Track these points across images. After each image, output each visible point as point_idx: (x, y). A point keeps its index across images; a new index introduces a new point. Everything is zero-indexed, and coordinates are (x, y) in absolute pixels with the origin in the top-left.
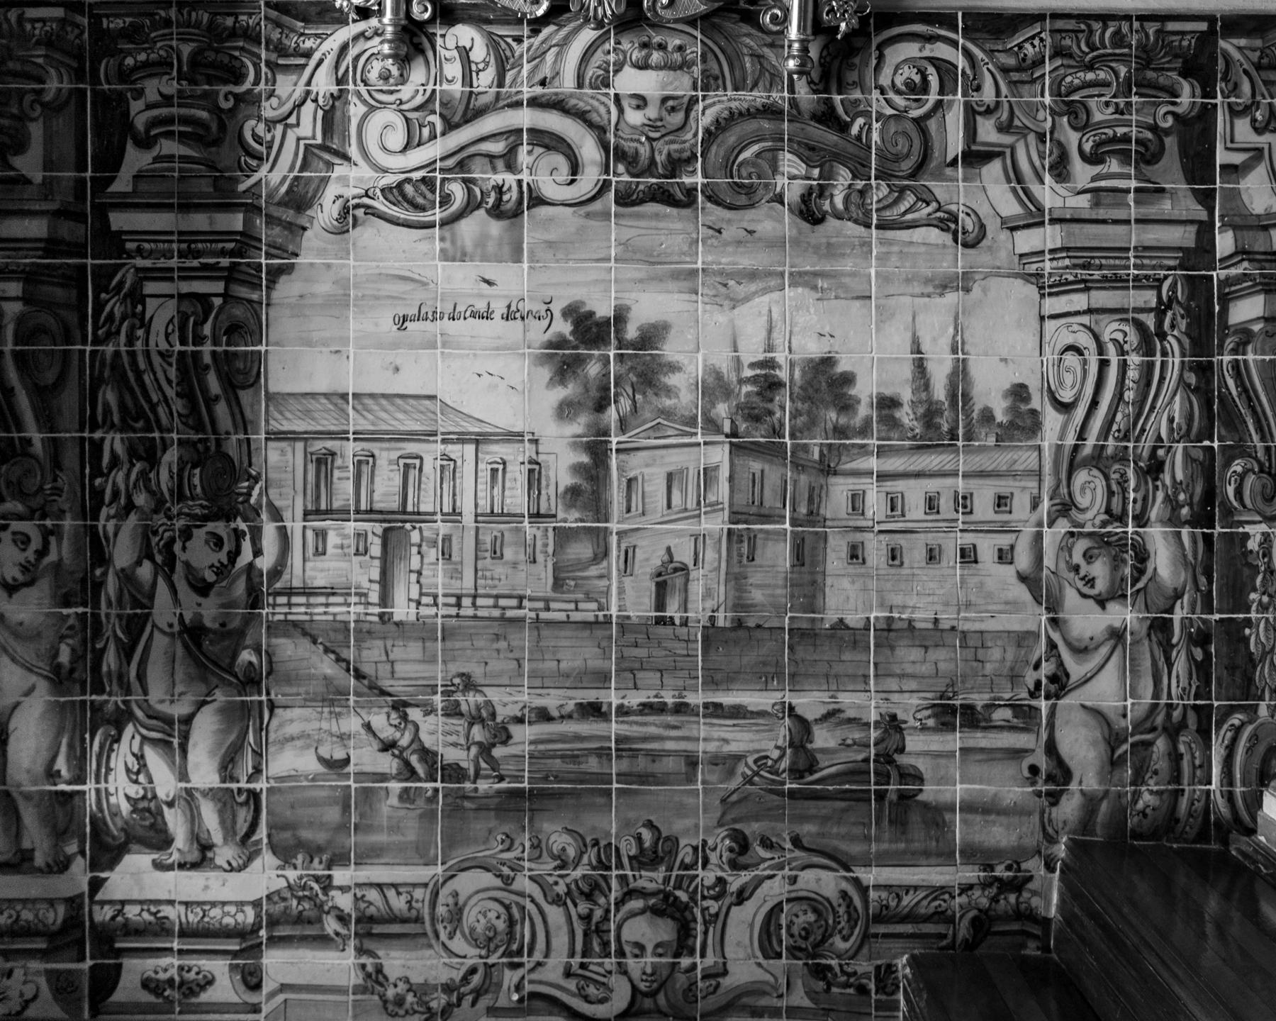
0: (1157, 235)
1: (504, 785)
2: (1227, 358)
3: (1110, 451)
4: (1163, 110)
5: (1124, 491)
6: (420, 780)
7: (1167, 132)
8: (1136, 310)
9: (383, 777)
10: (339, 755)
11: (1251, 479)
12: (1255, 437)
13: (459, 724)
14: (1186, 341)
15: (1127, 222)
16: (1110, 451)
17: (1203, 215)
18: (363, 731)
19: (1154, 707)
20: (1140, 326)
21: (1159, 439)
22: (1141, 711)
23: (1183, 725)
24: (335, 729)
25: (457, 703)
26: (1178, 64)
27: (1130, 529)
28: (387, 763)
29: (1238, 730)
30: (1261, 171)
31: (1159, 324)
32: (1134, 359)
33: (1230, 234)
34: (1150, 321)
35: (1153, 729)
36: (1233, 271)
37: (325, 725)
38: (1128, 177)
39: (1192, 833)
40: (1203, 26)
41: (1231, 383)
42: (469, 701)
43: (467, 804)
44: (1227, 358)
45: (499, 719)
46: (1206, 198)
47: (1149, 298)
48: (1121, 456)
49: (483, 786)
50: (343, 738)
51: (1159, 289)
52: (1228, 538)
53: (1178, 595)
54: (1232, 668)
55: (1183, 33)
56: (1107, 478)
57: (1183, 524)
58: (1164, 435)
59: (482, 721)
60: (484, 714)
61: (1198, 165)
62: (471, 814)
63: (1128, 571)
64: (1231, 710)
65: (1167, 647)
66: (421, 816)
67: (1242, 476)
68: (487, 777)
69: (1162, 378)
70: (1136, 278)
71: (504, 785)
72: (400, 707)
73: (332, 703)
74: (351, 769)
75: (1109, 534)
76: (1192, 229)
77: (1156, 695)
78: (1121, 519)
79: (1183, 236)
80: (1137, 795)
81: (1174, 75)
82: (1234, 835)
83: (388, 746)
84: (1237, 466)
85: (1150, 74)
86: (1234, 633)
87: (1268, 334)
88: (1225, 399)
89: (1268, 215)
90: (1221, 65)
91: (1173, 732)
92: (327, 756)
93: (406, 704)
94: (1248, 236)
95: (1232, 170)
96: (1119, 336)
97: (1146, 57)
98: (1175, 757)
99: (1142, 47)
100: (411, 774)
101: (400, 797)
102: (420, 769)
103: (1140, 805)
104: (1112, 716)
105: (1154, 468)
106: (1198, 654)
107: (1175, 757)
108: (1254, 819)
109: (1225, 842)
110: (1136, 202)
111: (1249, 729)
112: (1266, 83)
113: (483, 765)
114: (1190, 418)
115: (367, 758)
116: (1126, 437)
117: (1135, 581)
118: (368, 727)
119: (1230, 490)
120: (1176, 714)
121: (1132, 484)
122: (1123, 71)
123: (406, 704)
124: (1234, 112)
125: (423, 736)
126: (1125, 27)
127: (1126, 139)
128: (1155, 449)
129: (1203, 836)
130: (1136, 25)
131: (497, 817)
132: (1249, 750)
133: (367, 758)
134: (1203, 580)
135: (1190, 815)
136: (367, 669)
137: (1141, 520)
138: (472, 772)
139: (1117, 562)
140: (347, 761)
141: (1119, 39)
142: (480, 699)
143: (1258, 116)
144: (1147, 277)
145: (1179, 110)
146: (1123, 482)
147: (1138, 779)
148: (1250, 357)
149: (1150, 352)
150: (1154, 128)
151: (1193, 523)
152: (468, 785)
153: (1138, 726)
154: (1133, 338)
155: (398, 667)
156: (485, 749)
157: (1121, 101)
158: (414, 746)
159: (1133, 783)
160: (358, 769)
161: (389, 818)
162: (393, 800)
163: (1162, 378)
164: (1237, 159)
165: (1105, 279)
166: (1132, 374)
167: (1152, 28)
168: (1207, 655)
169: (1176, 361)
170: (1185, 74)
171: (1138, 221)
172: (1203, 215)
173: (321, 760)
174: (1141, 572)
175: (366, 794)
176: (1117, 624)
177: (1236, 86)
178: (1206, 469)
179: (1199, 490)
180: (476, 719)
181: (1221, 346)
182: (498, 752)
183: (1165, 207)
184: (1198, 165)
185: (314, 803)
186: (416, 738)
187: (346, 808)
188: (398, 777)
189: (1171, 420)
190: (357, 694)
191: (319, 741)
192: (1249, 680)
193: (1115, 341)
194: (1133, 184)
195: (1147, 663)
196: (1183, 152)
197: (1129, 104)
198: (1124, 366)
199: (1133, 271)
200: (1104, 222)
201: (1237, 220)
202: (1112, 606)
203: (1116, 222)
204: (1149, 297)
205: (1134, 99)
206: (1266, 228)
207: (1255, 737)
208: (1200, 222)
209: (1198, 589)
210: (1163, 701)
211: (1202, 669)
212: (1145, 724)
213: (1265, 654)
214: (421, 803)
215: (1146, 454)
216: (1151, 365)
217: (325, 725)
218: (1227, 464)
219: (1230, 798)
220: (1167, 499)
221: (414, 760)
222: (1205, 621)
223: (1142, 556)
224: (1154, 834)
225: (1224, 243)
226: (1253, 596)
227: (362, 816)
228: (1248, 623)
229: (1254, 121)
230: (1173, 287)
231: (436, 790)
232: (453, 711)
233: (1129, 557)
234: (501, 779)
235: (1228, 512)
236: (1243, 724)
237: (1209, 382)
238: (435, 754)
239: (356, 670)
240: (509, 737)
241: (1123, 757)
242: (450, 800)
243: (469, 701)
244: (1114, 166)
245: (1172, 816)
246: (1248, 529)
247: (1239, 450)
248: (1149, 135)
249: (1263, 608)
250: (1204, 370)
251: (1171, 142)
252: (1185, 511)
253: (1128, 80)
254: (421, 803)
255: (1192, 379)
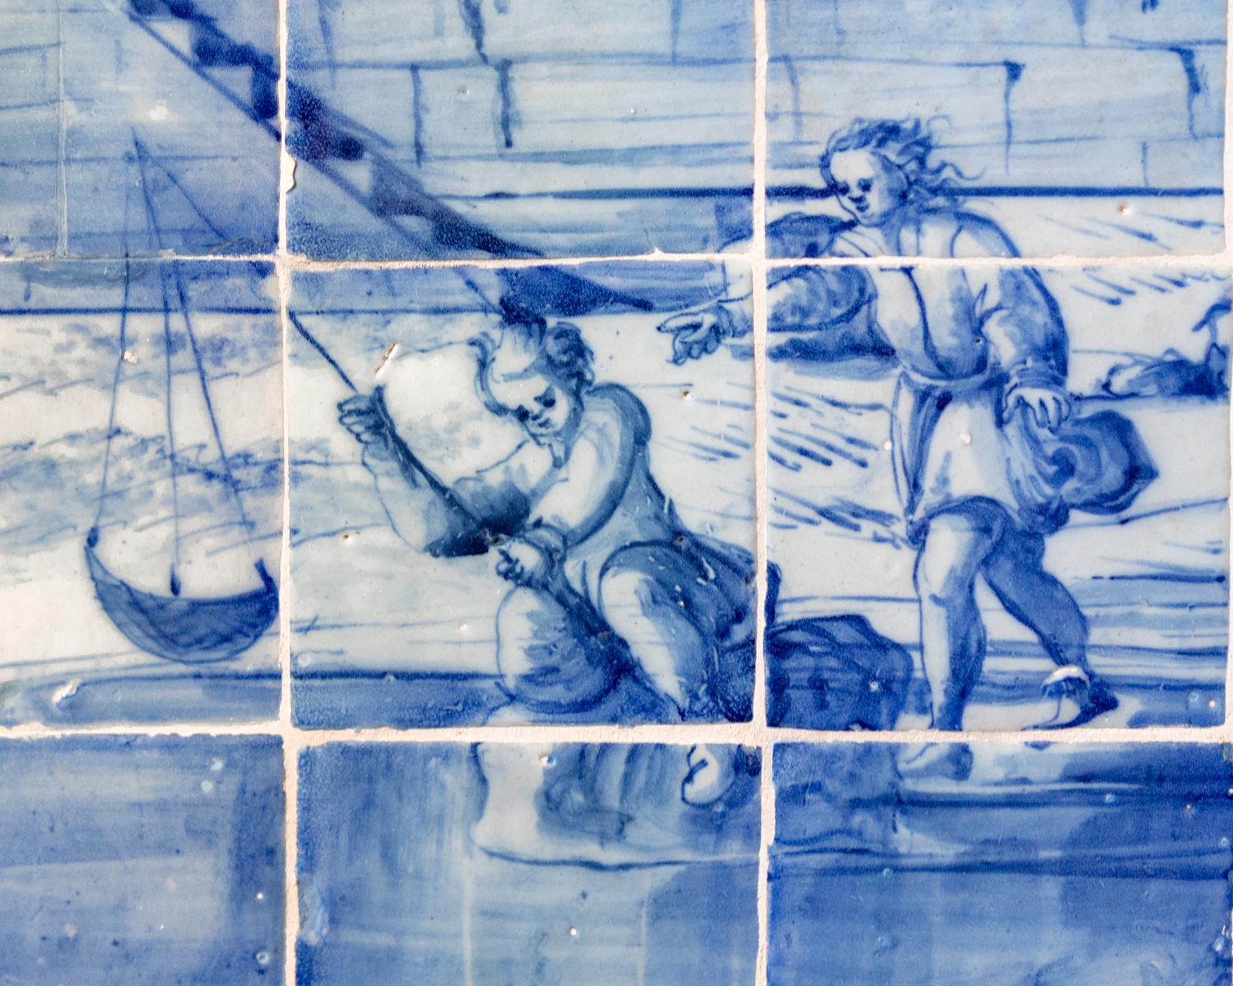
1: (1109, 735)
6: (652, 707)
9: (454, 695)
10: (217, 573)
13: (872, 402)
18: (343, 445)
24: (190, 430)
25: (858, 291)
28: (482, 620)
37: (139, 413)
42: (923, 276)
43: (913, 840)
45: (1084, 375)
49: (1001, 739)
50: (235, 478)
59: (994, 383)
60: (1004, 346)
62: (936, 896)
66: (663, 906)
68: (1020, 691)
71: (1109, 735)
72: (547, 305)
73: (175, 289)
74: (280, 647)
83: (482, 527)
92: (152, 582)
93: (579, 296)
100: (613, 677)
101: (551, 804)
102: (658, 650)
113: (999, 624)
115: (370, 590)
118: (372, 418)
123: (579, 296)
125: (670, 465)
131: (1076, 910)
133: (370, 590)
136: (361, 102)
138: (936, 665)
140: (261, 605)
142: (982, 264)
152: (915, 736)
155: (535, 93)
156: (1010, 541)
158: (626, 524)
160: (320, 650)
161: (490, 913)
162: (514, 821)
173: (119, 600)
175: (364, 789)
180: (958, 376)
182: (1080, 553)
185: (77, 838)
186: (634, 476)
187: (254, 862)
188: (537, 694)
190: (316, 240)
191: (108, 498)
214: (660, 832)
217: (139, 413)
221: (623, 598)
227: (340, 906)
231: (744, 765)
232: (837, 334)
234: (1097, 700)
238: (737, 566)
239: (307, 108)
240: (1139, 472)
242: (817, 817)
243: (923, 276)
254: (660, 832)
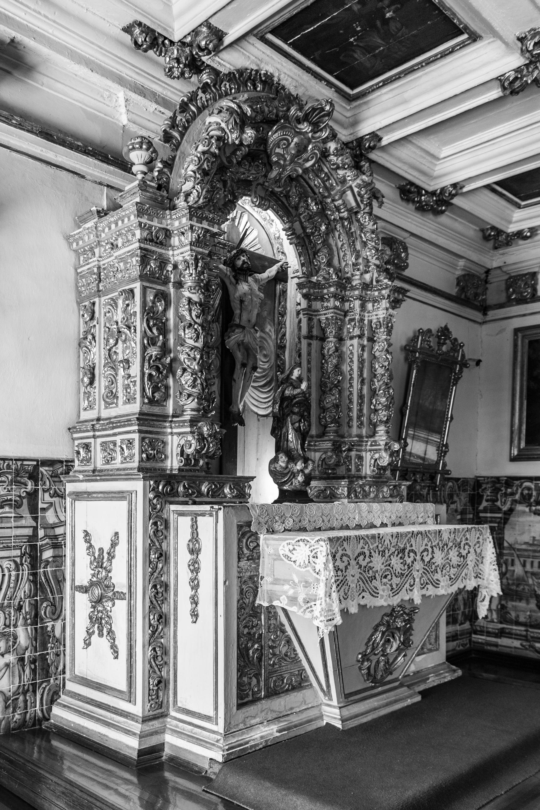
0: (20, 532)
2: (42, 570)
3: (5, 604)
4: (23, 490)
5: (10, 617)
7: (24, 498)
8: (14, 557)
11: (49, 608)
12: (50, 595)
14: (29, 566)
15: (11, 528)
16: (5, 604)
17: (35, 525)
19: (19, 686)
20: (15, 562)
21: (21, 598)
22: (15, 689)
23: (28, 690)
26: (27, 475)
27: (12, 629)
29: (44, 688)
30: (52, 510)
31: (21, 561)
32: (13, 573)
33: (43, 530)
34: (18, 560)
35: (19, 694)
36: (44, 542)
38: (11, 513)
39: (30, 724)
40: (35, 463)
41: (43, 578)
44: (42, 570)
46: (35, 519)
47: (18, 553)
48: (9, 606)
51: (21, 549)
52: (42, 628)
53: (27, 649)
54: (43, 669)
55: (29, 465)
56: (4, 613)
57: (28, 625)
58: (23, 597)
61: (34, 509)
63: (11, 643)
64: (43, 682)
65: (23, 666)
67: (46, 608)
69: (22, 579)
70: (14, 546)
75: (5, 632)
76: (32, 529)
77: (20, 682)
78: (9, 626)
79: (29, 532)
80: (14, 716)
81: (26, 479)
82: (43, 722)
84: (45, 605)
85: (19, 479)
86: (43, 658)
87: (54, 562)
88: (41, 584)
89: (54, 524)
90: (40, 476)
91: (25, 693)
94: (48, 530)
95: (43, 510)
96: (9, 566)
97: (17, 473)
98: (26, 701)
99: (16, 470)
103: (15, 719)
104: (6, 692)
105: (20, 608)
106: (33, 666)
107: (26, 701)
108: (49, 716)
109: (41, 725)
110: (14, 521)
111: (48, 687)
112: (54, 482)
114: (30, 591)
116: (11, 599)
117: (13, 646)
119: (43, 612)
120: (26, 687)
121: (12, 614)
122: (10, 477)
124: (44, 491)
126: (11, 463)
127: (11, 500)
128: (20, 602)
129: (34, 725)
130: (14, 462)
132: (48, 694)
134: (34, 642)
135: (30, 719)
137: (15, 626)
139: (7, 641)
141: (9, 467)
143: (51, 492)
144: (17, 546)
145: (27, 490)
146: (10, 614)
147: (14, 711)
148: (49, 569)
149: (18, 570)
150: (20, 496)
151: (31, 625)
153: (14, 694)
154: (13, 566)
157: (9, 487)
159: (13, 713)
163: (22, 579)
164: (45, 506)
165: (4, 547)
166: (13, 578)
167: (19, 463)
168: (35, 666)
169: (26, 572)
170: (29, 478)
171: (15, 527)
172: (35, 525)
174: (15, 643)
176: (8, 661)
177: (45, 483)
178: (35, 606)
179: (33, 613)
181: (40, 566)
183: (23, 522)
184: (34, 509)
189: (25, 592)
192: (48, 672)
193: (7, 567)
194: (13, 515)
195: (17, 673)
196: (29, 504)
197: (12, 488)
198: (10, 576)
199: (13, 544)
200: (4, 528)
201: (45, 526)
202: (6, 656)
203: (7, 528)
204: (18, 553)
205: (14, 487)
206: (53, 528)
207: (49, 689)
208: (34, 527)
209: (33, 646)
210: (22, 684)
211: (34, 671)
212: (16, 693)
213: (52, 663)
215: (17, 604)
216: (18, 575)
218: (42, 604)
219: (42, 711)
220: (24, 618)
222: (35, 656)
223: (16, 638)
224: (19, 728)
225: (41, 533)
226: (49, 645)
228: (48, 654)
229: (50, 493)
230: (25, 549)
233: (11, 639)
235: (42, 619)
236: (46, 686)
237: (36, 578)
241: (9, 705)
244: (7, 509)
245: (25, 721)
246: (48, 624)
247: (46, 599)
248: (18, 499)
249: (52, 648)
250: (35, 575)
251: (25, 501)
252: (29, 621)
253: (12, 480)
255: (31, 578)
